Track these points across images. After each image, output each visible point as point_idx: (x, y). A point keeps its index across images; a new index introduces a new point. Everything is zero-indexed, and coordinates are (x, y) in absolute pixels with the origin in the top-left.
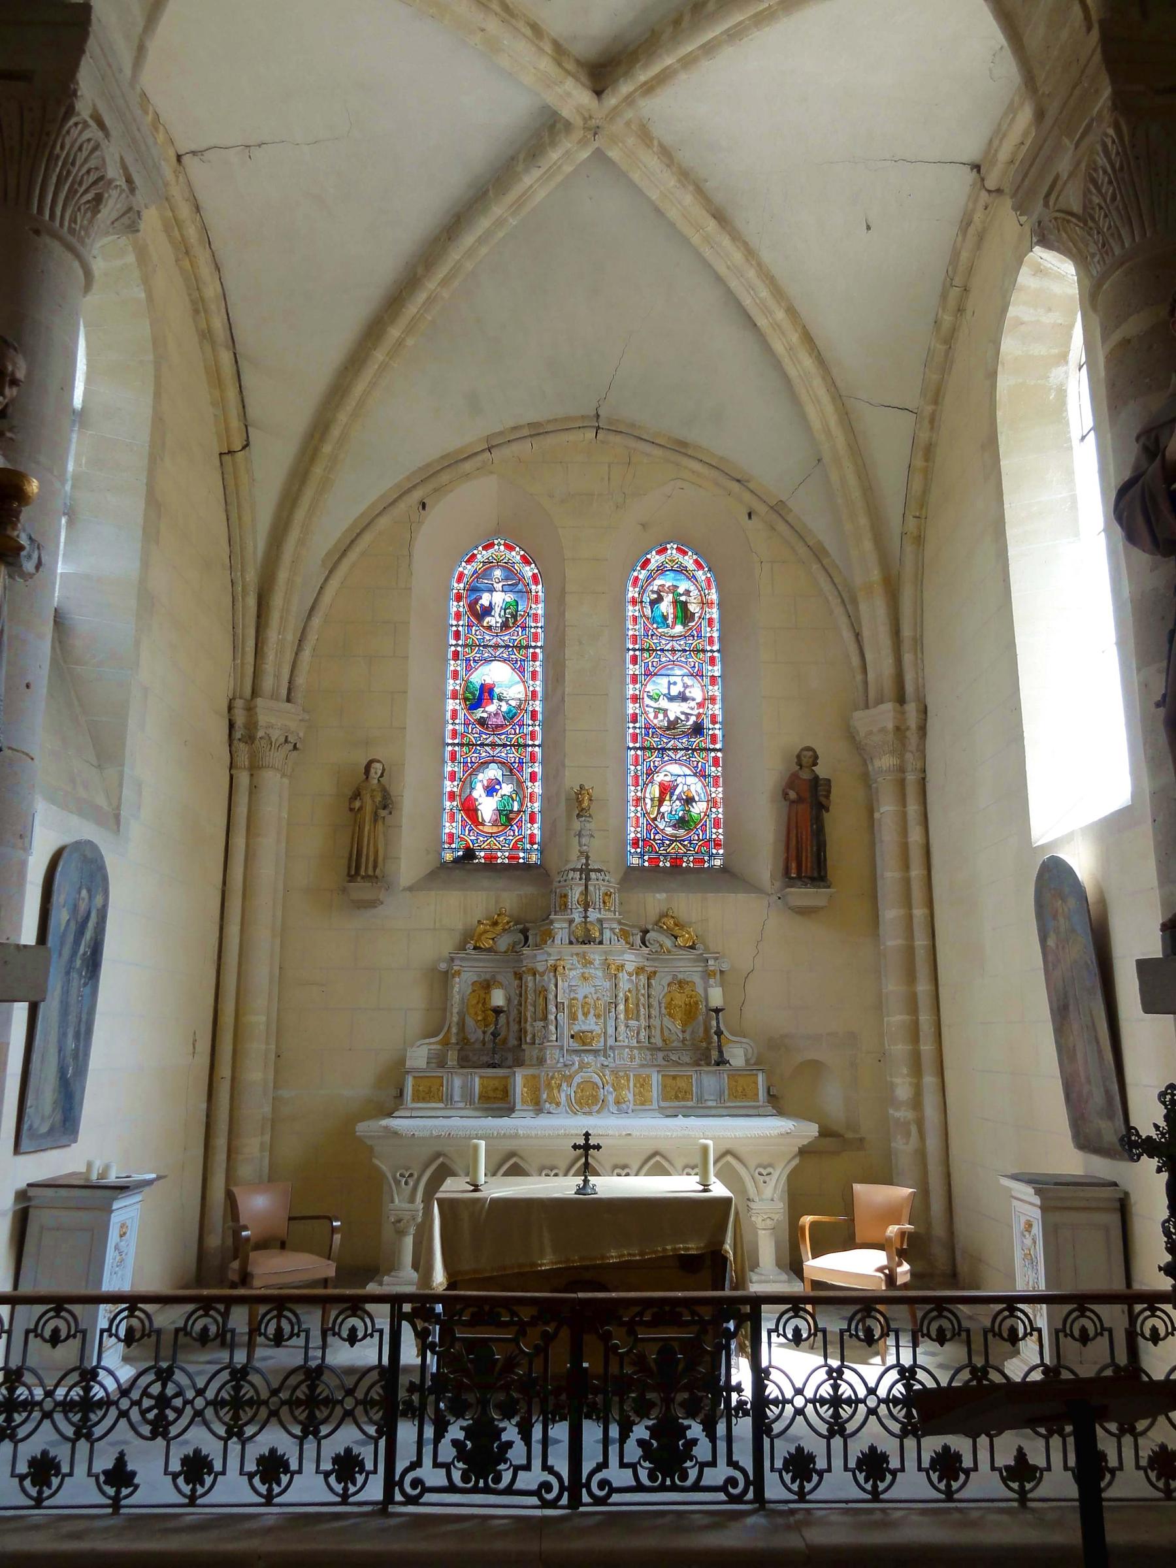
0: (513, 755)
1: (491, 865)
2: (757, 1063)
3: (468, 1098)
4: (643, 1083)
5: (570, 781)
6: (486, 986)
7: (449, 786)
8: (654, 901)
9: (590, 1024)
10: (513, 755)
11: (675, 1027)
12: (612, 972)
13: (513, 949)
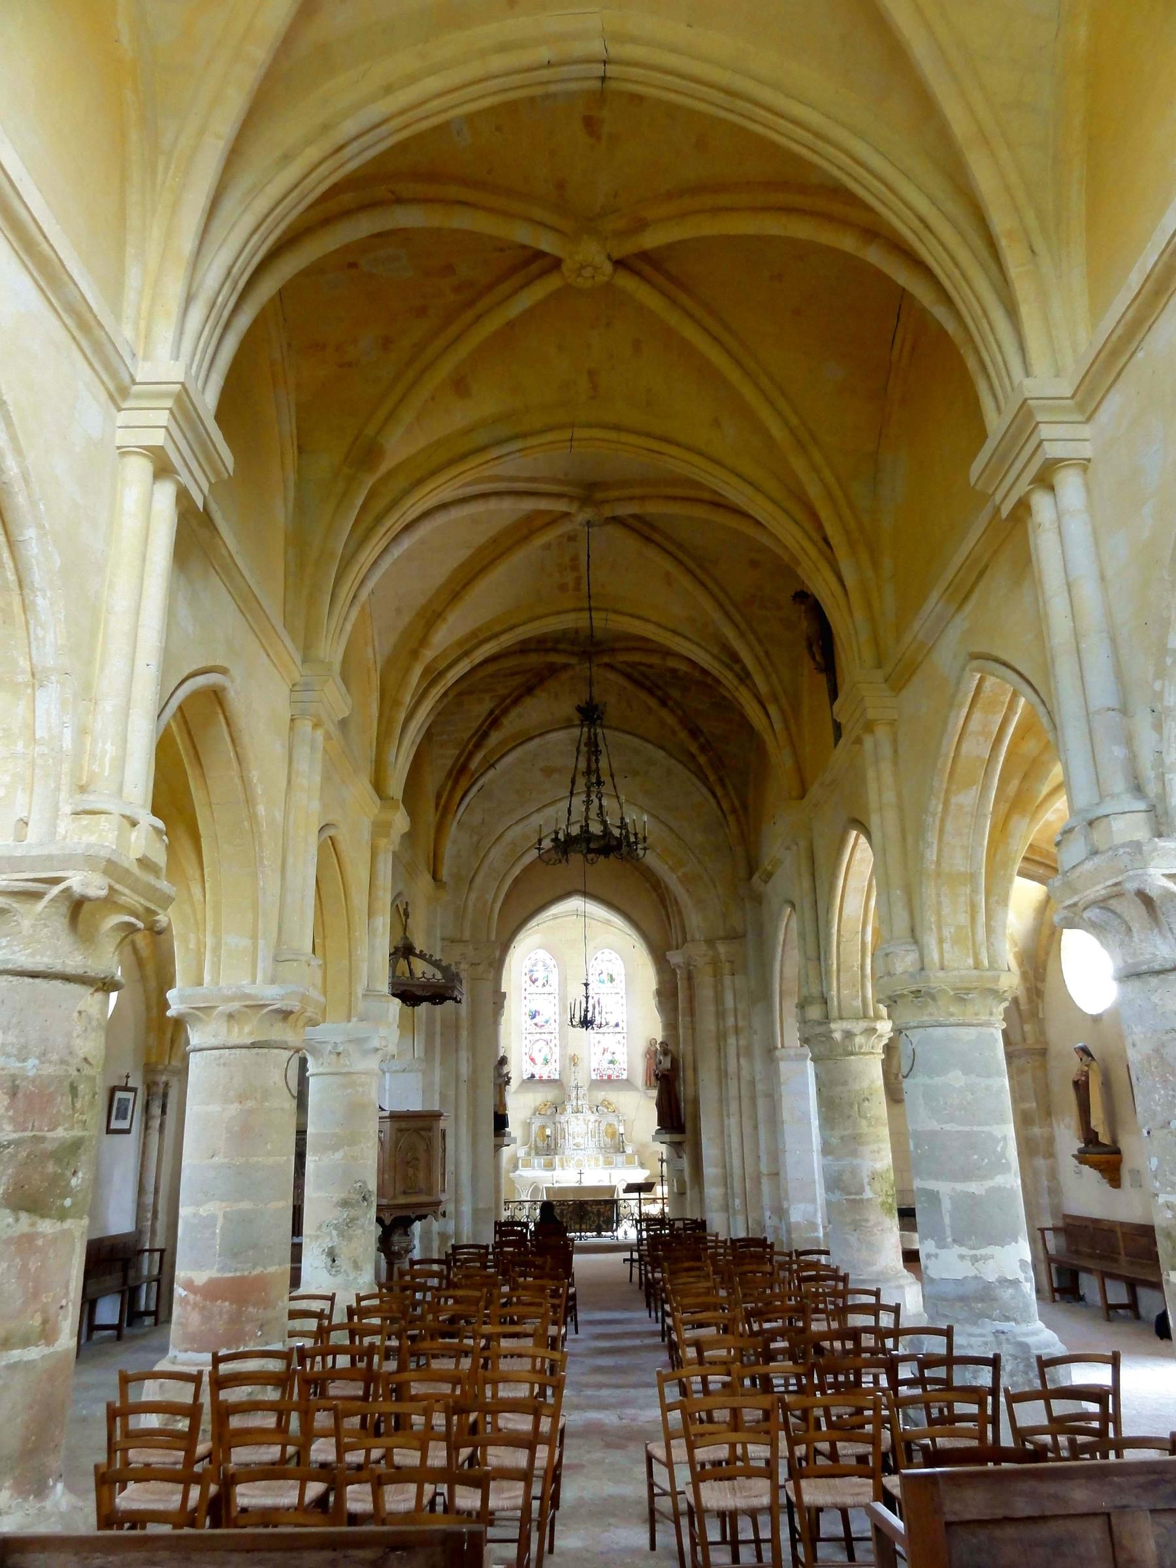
1: (541, 1081)
4: (597, 1160)
5: (570, 1052)
6: (543, 1127)
7: (525, 1050)
8: (601, 1095)
9: (579, 1140)
11: (608, 1140)
12: (587, 1122)
13: (552, 1114)
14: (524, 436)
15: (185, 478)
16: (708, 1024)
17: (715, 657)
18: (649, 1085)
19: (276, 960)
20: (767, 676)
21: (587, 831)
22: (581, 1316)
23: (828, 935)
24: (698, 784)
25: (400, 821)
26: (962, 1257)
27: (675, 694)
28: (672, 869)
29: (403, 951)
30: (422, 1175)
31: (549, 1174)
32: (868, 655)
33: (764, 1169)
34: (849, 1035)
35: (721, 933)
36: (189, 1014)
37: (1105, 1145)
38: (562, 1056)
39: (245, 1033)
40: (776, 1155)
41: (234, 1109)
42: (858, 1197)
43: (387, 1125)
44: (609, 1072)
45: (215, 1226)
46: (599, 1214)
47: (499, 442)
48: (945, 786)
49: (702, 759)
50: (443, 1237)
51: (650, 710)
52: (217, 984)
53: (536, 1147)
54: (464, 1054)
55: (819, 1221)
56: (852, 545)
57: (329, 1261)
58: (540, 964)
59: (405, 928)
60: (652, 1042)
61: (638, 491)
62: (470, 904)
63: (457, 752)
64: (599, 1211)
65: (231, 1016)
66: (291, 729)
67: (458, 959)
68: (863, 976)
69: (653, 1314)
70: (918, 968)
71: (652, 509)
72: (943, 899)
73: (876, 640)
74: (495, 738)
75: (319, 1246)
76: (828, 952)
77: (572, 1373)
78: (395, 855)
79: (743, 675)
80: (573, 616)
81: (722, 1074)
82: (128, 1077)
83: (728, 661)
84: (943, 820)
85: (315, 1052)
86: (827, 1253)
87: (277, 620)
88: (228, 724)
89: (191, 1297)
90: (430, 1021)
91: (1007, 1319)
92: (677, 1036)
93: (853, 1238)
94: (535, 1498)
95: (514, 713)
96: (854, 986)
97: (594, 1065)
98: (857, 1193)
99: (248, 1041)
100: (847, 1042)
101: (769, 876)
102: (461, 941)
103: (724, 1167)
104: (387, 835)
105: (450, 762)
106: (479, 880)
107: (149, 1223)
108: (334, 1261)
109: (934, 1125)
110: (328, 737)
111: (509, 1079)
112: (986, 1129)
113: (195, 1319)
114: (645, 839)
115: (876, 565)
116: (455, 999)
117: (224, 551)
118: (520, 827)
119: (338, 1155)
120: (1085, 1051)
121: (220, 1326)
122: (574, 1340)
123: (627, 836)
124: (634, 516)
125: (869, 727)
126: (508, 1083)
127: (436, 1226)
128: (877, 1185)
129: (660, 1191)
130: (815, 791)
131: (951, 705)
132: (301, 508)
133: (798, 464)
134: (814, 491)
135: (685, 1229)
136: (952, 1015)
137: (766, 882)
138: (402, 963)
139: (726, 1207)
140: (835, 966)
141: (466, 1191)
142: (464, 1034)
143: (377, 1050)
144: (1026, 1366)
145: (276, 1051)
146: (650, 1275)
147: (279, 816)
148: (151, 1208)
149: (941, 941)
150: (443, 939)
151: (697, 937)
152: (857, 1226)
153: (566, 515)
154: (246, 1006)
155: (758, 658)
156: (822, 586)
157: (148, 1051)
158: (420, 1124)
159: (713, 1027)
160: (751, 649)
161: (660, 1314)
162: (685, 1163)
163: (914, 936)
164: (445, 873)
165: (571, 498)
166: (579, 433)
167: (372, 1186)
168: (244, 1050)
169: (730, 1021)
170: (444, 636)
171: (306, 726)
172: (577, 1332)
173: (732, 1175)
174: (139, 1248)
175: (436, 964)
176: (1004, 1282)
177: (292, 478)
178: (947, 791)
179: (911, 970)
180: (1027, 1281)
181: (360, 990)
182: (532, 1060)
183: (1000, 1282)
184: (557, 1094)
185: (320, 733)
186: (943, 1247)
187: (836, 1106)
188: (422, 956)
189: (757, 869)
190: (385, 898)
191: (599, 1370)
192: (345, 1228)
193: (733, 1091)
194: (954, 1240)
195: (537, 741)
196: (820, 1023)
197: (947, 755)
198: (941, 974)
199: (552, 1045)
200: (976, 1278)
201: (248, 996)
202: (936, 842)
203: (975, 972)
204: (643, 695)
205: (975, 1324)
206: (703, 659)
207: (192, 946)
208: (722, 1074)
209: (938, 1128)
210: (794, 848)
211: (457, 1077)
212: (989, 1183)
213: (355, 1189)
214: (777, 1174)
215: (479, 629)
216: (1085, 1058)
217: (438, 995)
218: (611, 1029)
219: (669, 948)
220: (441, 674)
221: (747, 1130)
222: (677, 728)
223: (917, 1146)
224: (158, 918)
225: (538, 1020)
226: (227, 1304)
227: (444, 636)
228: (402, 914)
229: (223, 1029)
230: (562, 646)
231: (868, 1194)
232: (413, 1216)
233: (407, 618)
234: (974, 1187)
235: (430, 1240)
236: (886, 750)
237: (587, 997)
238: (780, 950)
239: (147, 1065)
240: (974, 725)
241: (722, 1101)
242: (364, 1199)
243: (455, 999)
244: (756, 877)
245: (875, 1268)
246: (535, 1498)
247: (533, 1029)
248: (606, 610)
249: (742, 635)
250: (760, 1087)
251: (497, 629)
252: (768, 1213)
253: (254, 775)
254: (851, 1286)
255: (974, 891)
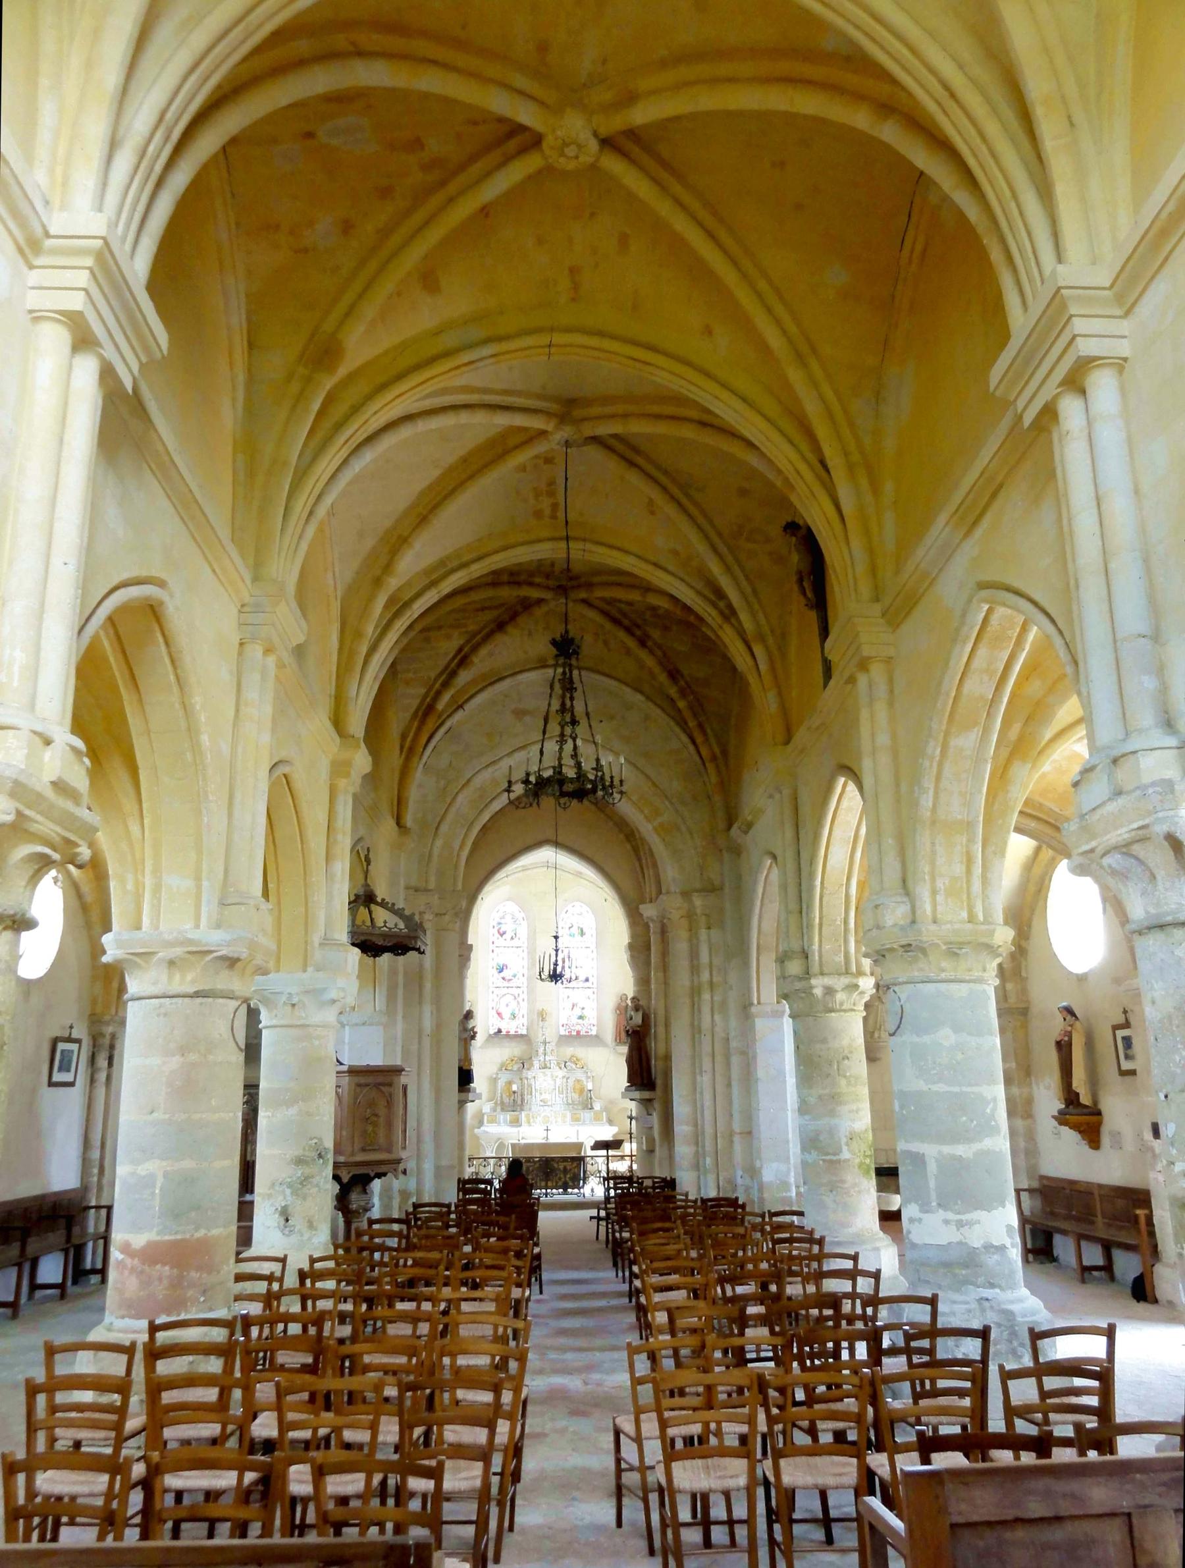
0: (515, 991)
1: (508, 1035)
2: (605, 1109)
3: (505, 1121)
4: (564, 1116)
6: (510, 1083)
8: (569, 1051)
9: (546, 1096)
10: (515, 991)
11: (576, 1096)
13: (518, 1070)
14: (500, 339)
15: (110, 353)
16: (682, 979)
17: (699, 593)
18: (619, 1041)
19: (223, 904)
20: (753, 615)
21: (560, 773)
22: (545, 1276)
23: (811, 888)
24: (677, 730)
25: (362, 761)
26: (947, 1222)
27: (656, 634)
28: (648, 819)
29: (364, 899)
30: (381, 1133)
31: (515, 1130)
32: (865, 589)
33: (737, 1127)
34: (829, 991)
35: (698, 885)
36: (126, 960)
37: (1086, 1107)
38: (530, 1011)
39: (186, 982)
40: (749, 1115)
41: (175, 1062)
42: (834, 1158)
43: (346, 1080)
44: (578, 1028)
45: (155, 1187)
46: (565, 1171)
47: (470, 346)
48: (944, 727)
49: (681, 704)
50: (405, 1194)
51: (628, 652)
52: (157, 928)
53: (502, 1103)
54: (427, 1010)
55: (792, 1180)
56: (851, 468)
57: (283, 1222)
58: (508, 917)
59: (366, 873)
60: (623, 997)
61: (620, 408)
62: (436, 852)
63: (423, 691)
64: (565, 1168)
65: (171, 963)
66: (240, 654)
67: (422, 908)
68: (846, 930)
69: (620, 1274)
70: (908, 921)
71: (636, 428)
72: (937, 847)
73: (873, 570)
74: (464, 677)
75: (272, 1205)
76: (810, 907)
77: (537, 1336)
78: (356, 798)
79: (727, 612)
80: (547, 546)
81: (695, 1030)
82: (71, 1027)
83: (713, 597)
84: (940, 765)
85: (267, 1002)
86: (801, 1214)
87: (224, 533)
88: (167, 644)
89: (129, 1261)
90: (393, 972)
91: (992, 1286)
92: (648, 992)
93: (828, 1200)
94: (495, 1474)
95: (483, 651)
96: (837, 940)
97: (563, 1020)
98: (834, 1154)
99: (191, 990)
100: (828, 997)
101: (750, 825)
102: (426, 890)
103: (696, 1125)
104: (348, 775)
105: (415, 703)
106: (444, 828)
107: (95, 1179)
108: (287, 1220)
109: (921, 1085)
110: (281, 666)
111: (475, 1033)
112: (975, 1089)
113: (132, 1285)
114: (621, 781)
115: (876, 489)
116: (418, 950)
117: (160, 448)
118: (490, 770)
119: (293, 1111)
120: (1069, 1011)
121: (160, 1291)
122: (538, 1301)
123: (602, 778)
124: (615, 436)
125: (863, 665)
126: (473, 1037)
127: (397, 1183)
128: (854, 1145)
129: (628, 1148)
130: (801, 736)
131: (954, 641)
132: (251, 412)
133: (795, 376)
134: (812, 408)
135: (654, 1188)
136: (943, 971)
137: (746, 833)
138: (363, 911)
139: (697, 1166)
140: (817, 920)
141: (428, 1146)
142: (428, 986)
143: (334, 1001)
144: (1010, 1334)
145: (221, 1000)
146: (617, 1235)
147: (225, 749)
148: (97, 1163)
149: (934, 892)
150: (407, 888)
151: (672, 889)
152: (833, 1187)
153: (543, 433)
154: (189, 953)
155: (742, 593)
156: (817, 515)
157: (94, 1002)
158: (380, 1079)
159: (687, 983)
160: (738, 584)
161: (627, 1274)
162: (655, 1120)
163: (905, 887)
164: (409, 821)
165: (548, 414)
166: (558, 338)
167: (329, 1143)
168: (186, 1000)
169: (705, 976)
170: (411, 563)
171: (255, 651)
172: (541, 1293)
173: (703, 1133)
174: (84, 1204)
175: (399, 913)
176: (989, 1248)
177: (241, 378)
178: (947, 734)
179: (902, 922)
180: (1013, 1246)
181: (316, 939)
182: (499, 1014)
183: (985, 1247)
184: (525, 1049)
185: (271, 660)
186: (927, 1212)
187: (813, 1063)
188: (383, 904)
189: (736, 819)
190: (345, 843)
191: (563, 1332)
192: (300, 1186)
193: (706, 1047)
194: (939, 1205)
195: (507, 683)
196: (800, 979)
197: (948, 695)
198: (933, 927)
199: (520, 999)
200: (960, 1243)
201: (190, 942)
202: (932, 786)
203: (969, 926)
204: (622, 635)
205: (958, 1290)
206: (687, 595)
207: (130, 887)
208: (695, 1030)
209: (925, 1088)
210: (777, 796)
211: (420, 1031)
212: (976, 1146)
213: (311, 1146)
214: (750, 1133)
215: (448, 558)
216: (1069, 1017)
217: (400, 946)
218: (581, 984)
219: (643, 902)
220: (407, 605)
221: (720, 1088)
222: (657, 670)
223: (902, 1107)
224: (79, 850)
225: (505, 973)
226: (167, 1268)
227: (411, 563)
228: (363, 859)
229: (164, 977)
230: (537, 580)
231: (846, 1155)
232: (372, 1174)
233: (370, 543)
234: (961, 1150)
235: (390, 1198)
236: (881, 689)
237: (557, 951)
238: (758, 903)
239: (92, 1015)
240: (977, 663)
241: (695, 1057)
242: (320, 1156)
243: (418, 950)
244: (735, 826)
245: (850, 1230)
246: (495, 1474)
247: (501, 983)
248: (584, 540)
249: (728, 569)
250: (734, 1044)
251: (465, 559)
252: (740, 1173)
253: (197, 701)
254: (827, 1250)
255: (971, 840)
